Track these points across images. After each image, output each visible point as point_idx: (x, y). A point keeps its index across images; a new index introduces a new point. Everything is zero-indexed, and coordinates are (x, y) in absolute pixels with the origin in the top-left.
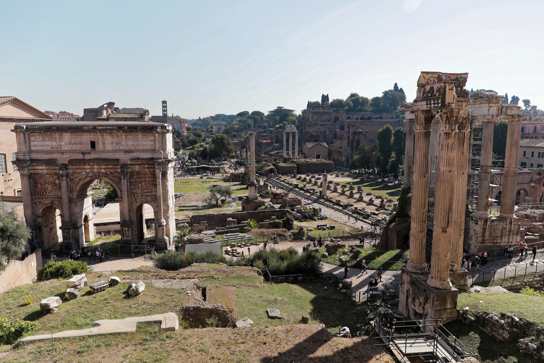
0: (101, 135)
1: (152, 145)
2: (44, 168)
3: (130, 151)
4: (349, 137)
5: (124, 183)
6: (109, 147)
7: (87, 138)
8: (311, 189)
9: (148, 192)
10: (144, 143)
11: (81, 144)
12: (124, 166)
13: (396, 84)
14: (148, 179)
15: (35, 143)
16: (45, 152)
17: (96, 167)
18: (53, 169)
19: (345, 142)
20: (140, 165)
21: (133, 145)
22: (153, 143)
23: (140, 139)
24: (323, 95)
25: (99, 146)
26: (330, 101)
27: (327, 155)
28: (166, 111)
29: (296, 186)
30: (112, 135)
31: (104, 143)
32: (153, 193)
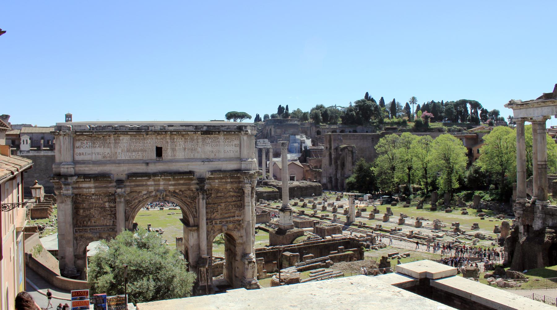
0: (171, 139)
2: (92, 185)
3: (209, 160)
4: (330, 155)
5: (202, 203)
6: (180, 155)
7: (152, 143)
9: (229, 217)
10: (227, 148)
11: (144, 151)
15: (81, 150)
16: (95, 163)
17: (162, 183)
18: (105, 187)
19: (325, 161)
20: (221, 178)
21: (212, 152)
22: (238, 149)
23: (222, 143)
25: (167, 154)
30: (185, 139)
31: (174, 150)
32: (236, 218)
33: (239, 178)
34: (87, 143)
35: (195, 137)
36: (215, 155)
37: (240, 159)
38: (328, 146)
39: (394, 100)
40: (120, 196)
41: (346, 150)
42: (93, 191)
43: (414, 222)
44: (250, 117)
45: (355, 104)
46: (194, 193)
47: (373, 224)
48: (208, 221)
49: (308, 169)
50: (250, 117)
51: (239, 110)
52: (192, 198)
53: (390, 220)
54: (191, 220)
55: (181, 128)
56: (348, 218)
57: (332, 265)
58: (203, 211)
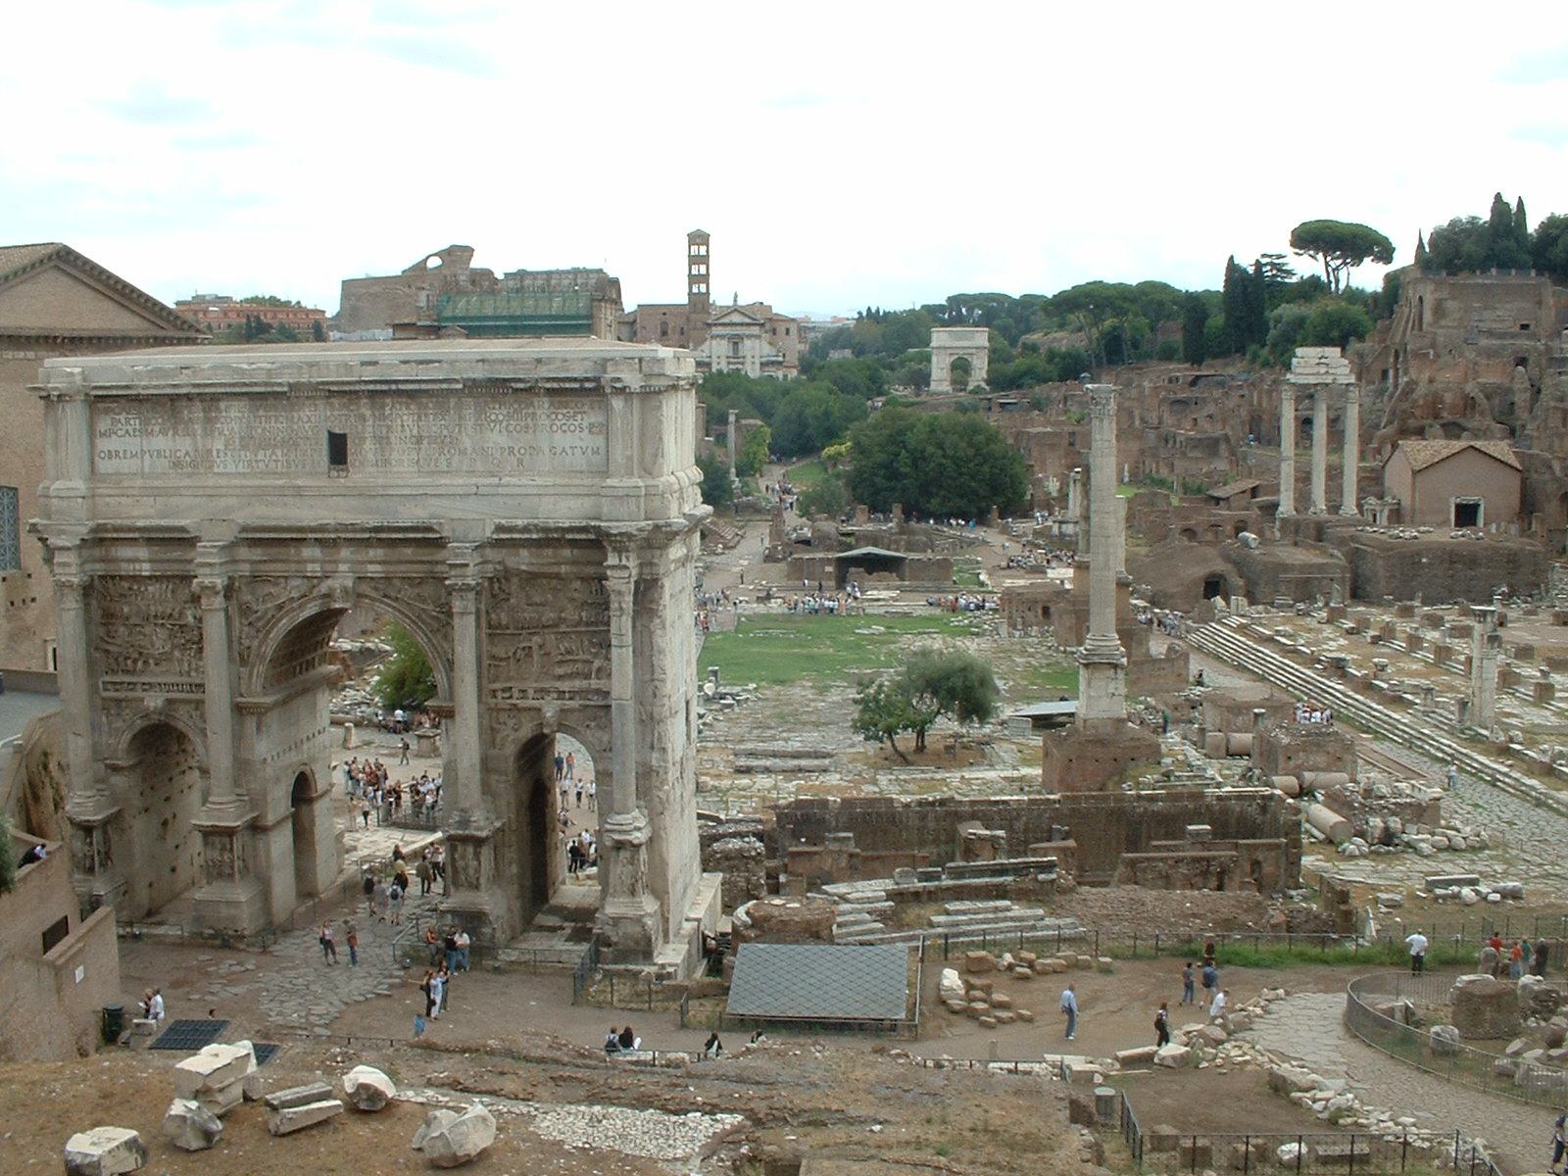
0: (372, 408)
1: (596, 452)
2: (143, 552)
7: (315, 421)
8: (1416, 690)
10: (562, 440)
11: (291, 443)
14: (571, 614)
21: (511, 450)
22: (600, 441)
23: (544, 421)
24: (1498, 197)
25: (363, 450)
26: (1532, 225)
27: (1515, 500)
28: (705, 278)
29: (1338, 668)
30: (420, 406)
31: (383, 441)
32: (594, 683)
36: (520, 462)
42: (146, 569)
48: (497, 686)
49: (1547, 477)
52: (441, 606)
57: (1063, 891)
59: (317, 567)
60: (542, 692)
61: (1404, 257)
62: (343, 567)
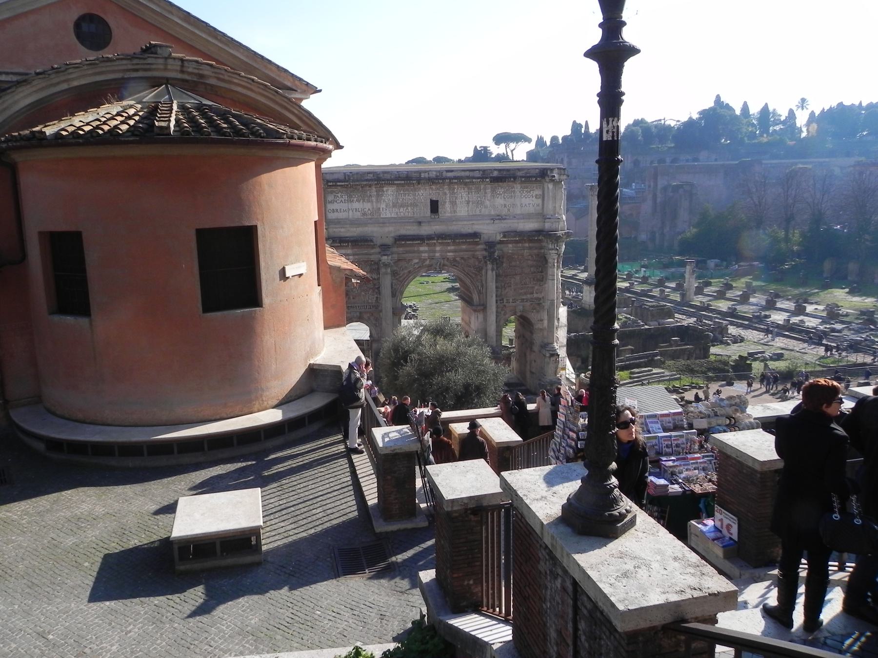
0: (449, 189)
1: (538, 205)
4: (655, 197)
6: (462, 211)
7: (425, 194)
9: (525, 294)
10: (525, 201)
11: (414, 205)
12: (491, 245)
13: (718, 97)
15: (335, 206)
16: (354, 223)
21: (505, 206)
22: (540, 201)
23: (518, 194)
24: (574, 122)
25: (446, 210)
30: (469, 189)
31: (453, 203)
32: (535, 295)
33: (540, 241)
34: (342, 197)
35: (482, 186)
36: (509, 210)
37: (543, 216)
38: (652, 184)
39: (766, 104)
40: (386, 265)
41: (681, 191)
43: (790, 305)
44: (529, 140)
45: (698, 116)
46: (480, 262)
47: (723, 306)
50: (529, 140)
51: (513, 130)
53: (752, 300)
54: (475, 297)
55: (463, 174)
56: (683, 296)
58: (492, 285)
59: (426, 255)
60: (514, 301)
61: (532, 146)
62: (437, 255)
